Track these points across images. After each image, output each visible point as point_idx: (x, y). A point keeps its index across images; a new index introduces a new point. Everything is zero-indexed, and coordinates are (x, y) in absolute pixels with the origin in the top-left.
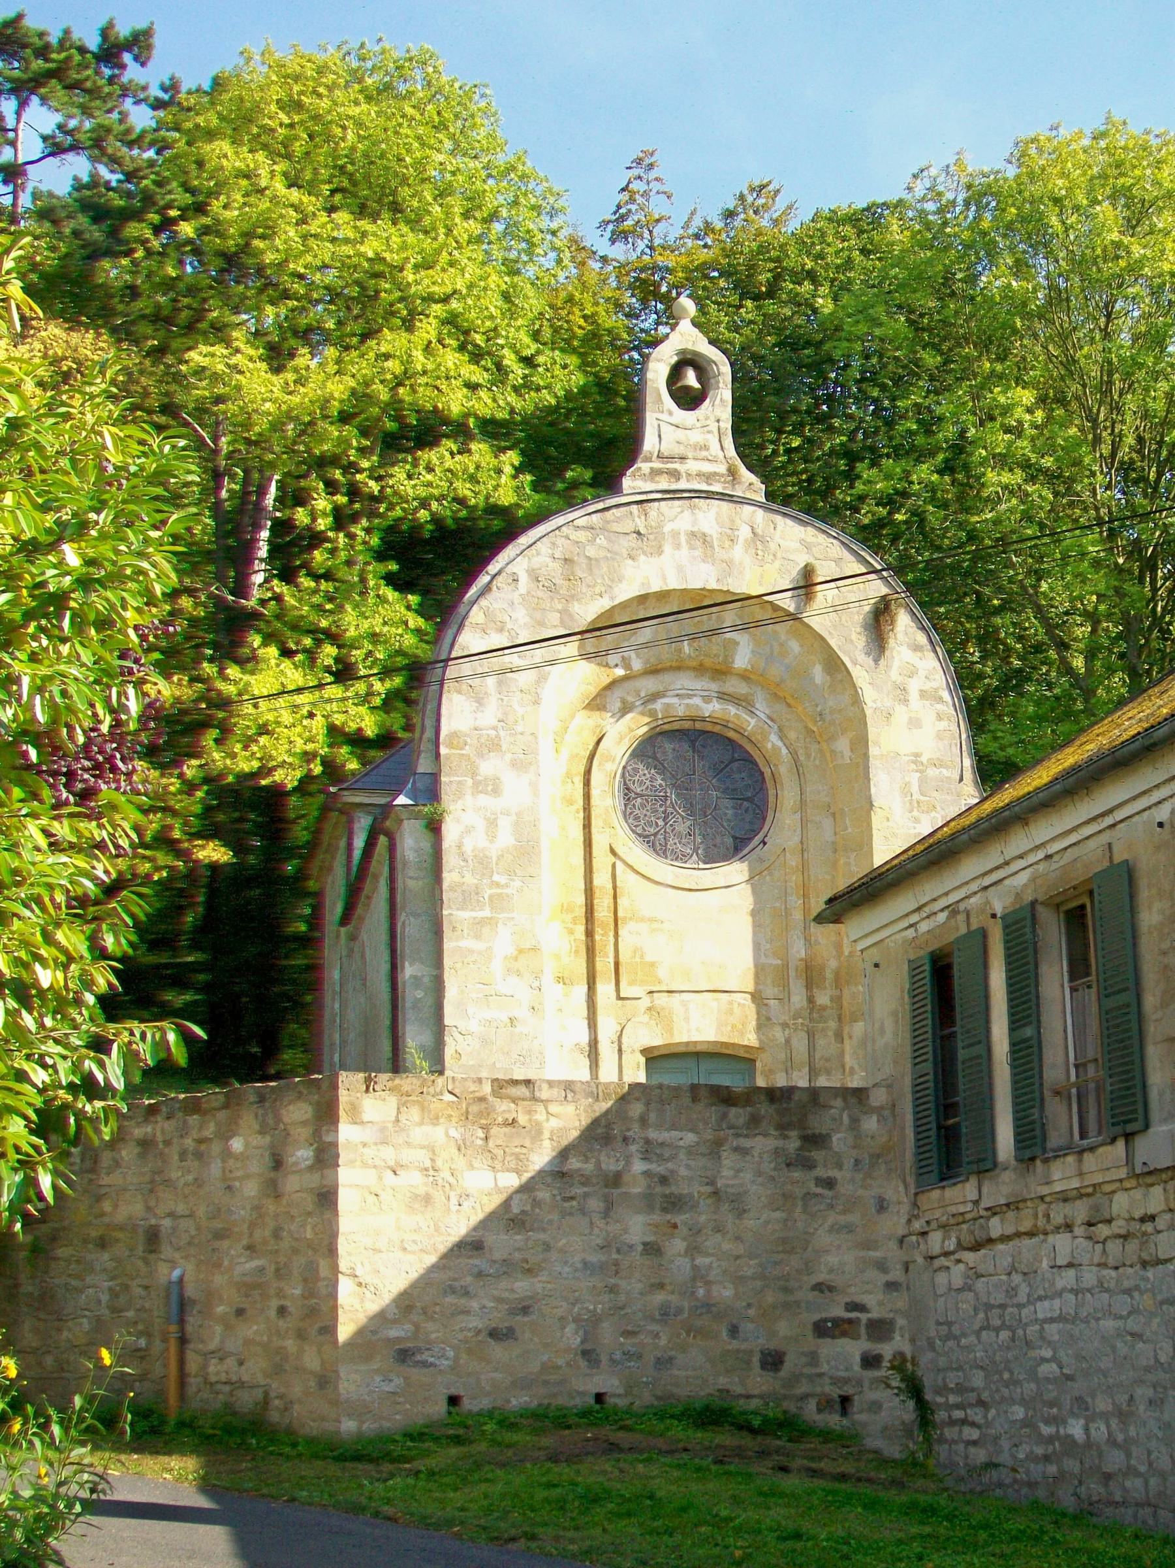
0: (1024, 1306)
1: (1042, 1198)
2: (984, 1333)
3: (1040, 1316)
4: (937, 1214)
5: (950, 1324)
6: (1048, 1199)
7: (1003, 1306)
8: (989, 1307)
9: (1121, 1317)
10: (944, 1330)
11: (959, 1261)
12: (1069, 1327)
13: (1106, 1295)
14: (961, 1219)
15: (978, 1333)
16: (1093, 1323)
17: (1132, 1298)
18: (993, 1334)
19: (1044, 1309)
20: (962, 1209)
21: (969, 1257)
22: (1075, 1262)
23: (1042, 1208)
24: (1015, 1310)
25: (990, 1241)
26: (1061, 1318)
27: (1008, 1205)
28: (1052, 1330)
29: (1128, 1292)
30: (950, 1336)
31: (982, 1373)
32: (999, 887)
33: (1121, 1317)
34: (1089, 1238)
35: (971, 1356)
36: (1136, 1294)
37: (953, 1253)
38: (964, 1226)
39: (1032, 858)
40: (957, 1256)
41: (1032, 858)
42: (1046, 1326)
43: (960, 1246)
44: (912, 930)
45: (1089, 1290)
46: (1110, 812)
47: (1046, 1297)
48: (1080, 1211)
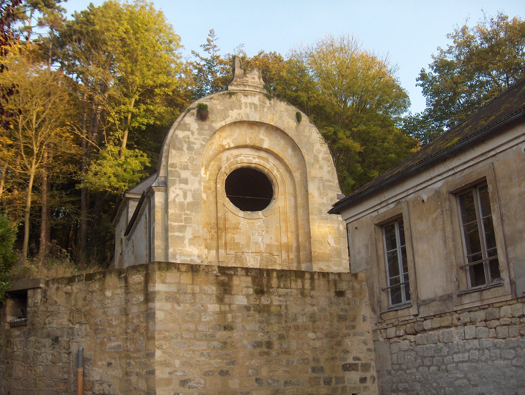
0: (446, 356)
1: (456, 311)
2: (420, 368)
3: (456, 360)
4: (393, 321)
5: (400, 365)
6: (458, 312)
7: (433, 357)
8: (424, 357)
9: (509, 359)
10: (397, 367)
11: (405, 339)
12: (474, 364)
13: (499, 351)
14: (406, 322)
15: (417, 368)
16: (490, 362)
17: (516, 351)
18: (426, 369)
19: (457, 358)
20: (407, 318)
21: (412, 338)
22: (478, 337)
23: (457, 315)
24: (440, 358)
25: (424, 331)
26: (469, 361)
27: (435, 316)
28: (465, 366)
29: (513, 348)
30: (400, 369)
31: (419, 384)
32: (426, 189)
33: (509, 359)
34: (486, 326)
35: (413, 377)
36: (519, 349)
37: (401, 336)
38: (408, 325)
39: (445, 176)
40: (404, 337)
41: (445, 176)
42: (460, 364)
43: (407, 334)
44: (376, 212)
45: (487, 349)
46: (453, 169)
47: (459, 353)
48: (481, 315)
